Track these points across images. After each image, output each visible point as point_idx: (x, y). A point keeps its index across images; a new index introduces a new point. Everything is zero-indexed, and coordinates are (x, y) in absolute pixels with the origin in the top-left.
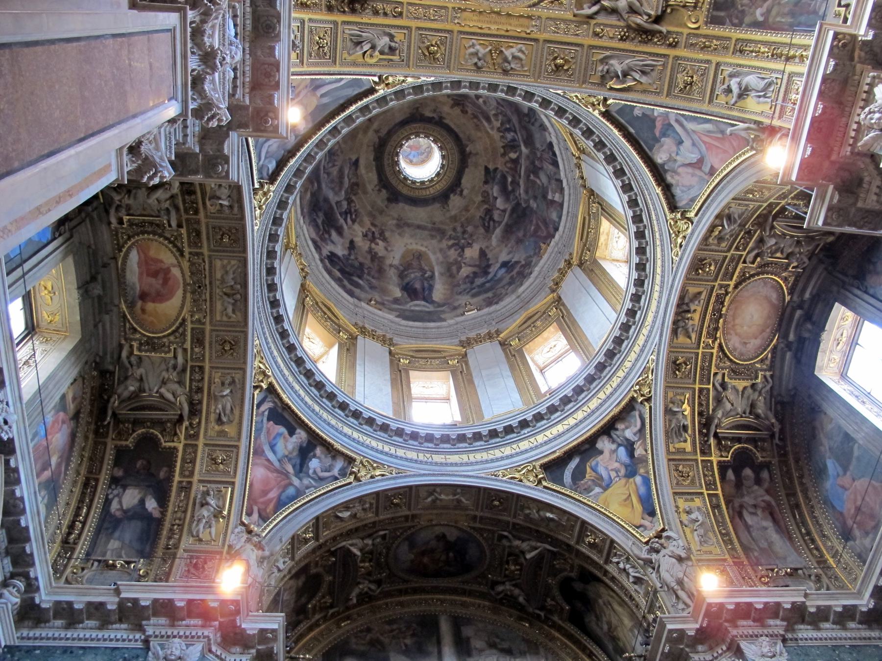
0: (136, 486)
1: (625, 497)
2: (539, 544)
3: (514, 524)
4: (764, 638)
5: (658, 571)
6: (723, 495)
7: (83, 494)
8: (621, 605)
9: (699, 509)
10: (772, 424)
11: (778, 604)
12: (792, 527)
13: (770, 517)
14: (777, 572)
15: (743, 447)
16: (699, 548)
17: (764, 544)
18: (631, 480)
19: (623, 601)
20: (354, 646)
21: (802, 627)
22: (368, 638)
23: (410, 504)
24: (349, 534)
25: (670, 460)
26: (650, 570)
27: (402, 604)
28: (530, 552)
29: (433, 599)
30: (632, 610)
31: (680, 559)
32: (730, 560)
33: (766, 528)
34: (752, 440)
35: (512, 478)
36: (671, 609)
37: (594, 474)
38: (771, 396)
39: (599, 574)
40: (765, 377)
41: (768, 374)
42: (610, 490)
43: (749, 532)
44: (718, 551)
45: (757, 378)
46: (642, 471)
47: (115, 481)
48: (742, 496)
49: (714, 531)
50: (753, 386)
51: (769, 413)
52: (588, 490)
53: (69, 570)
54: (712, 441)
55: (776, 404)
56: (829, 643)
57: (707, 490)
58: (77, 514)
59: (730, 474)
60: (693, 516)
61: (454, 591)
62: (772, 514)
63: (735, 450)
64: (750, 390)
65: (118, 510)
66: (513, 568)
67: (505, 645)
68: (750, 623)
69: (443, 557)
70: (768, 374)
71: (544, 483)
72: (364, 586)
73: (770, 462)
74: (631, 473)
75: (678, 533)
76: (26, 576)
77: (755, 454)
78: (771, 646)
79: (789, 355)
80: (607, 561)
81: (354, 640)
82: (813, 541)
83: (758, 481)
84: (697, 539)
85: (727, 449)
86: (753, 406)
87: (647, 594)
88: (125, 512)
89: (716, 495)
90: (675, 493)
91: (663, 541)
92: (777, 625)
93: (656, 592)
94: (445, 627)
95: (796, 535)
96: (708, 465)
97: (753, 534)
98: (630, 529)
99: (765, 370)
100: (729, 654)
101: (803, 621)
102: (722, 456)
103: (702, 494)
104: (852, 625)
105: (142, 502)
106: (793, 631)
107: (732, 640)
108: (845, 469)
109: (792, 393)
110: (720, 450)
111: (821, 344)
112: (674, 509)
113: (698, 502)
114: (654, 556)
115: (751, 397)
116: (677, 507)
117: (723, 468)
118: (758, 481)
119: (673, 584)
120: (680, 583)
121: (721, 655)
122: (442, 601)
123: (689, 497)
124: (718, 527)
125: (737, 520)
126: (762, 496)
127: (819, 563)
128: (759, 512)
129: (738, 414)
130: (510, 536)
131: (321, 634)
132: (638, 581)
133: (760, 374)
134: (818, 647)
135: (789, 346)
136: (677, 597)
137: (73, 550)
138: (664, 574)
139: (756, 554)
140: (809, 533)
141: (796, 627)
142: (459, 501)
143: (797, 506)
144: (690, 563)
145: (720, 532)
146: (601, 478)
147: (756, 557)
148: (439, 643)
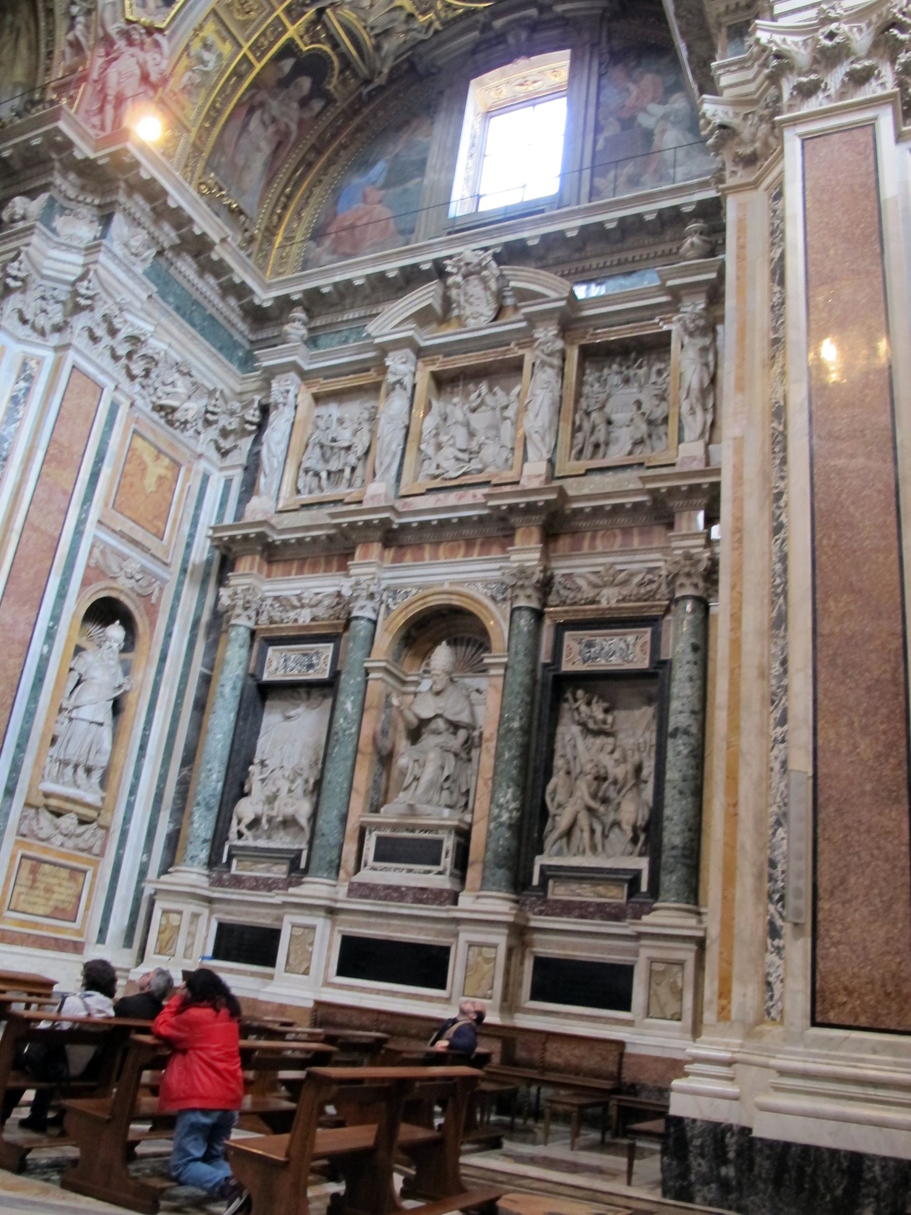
4: (145, 232)
5: (109, 63)
6: (258, 74)
8: (30, 48)
9: (220, 56)
10: (380, 73)
11: (190, 221)
12: (282, 176)
13: (274, 146)
14: (222, 196)
15: (329, 57)
16: (176, 90)
17: (240, 161)
19: (38, 48)
26: (101, 51)
30: (37, 68)
31: (145, 78)
32: (193, 135)
33: (259, 149)
34: (346, 62)
36: (82, 112)
38: (412, 48)
40: (431, 24)
41: (437, 25)
43: (240, 135)
44: (192, 115)
45: (424, 13)
48: (274, 96)
49: (209, 95)
50: (411, 16)
51: (391, 58)
54: (311, 12)
55: (408, 60)
57: (250, 48)
59: (288, 65)
60: (207, 56)
62: (279, 145)
63: (320, 49)
64: (402, 16)
68: (148, 208)
70: (437, 25)
73: (335, 101)
75: (173, 52)
77: (332, 76)
78: (143, 245)
79: (475, 34)
82: (285, 207)
83: (304, 103)
84: (185, 80)
85: (315, 39)
86: (387, 33)
87: (72, 70)
89: (251, 66)
90: (214, 12)
91: (148, 40)
92: (169, 235)
93: (84, 78)
95: (276, 186)
96: (278, 28)
97: (242, 141)
99: (439, 18)
100: (95, 211)
101: (196, 256)
102: (301, 37)
106: (178, 255)
107: (113, 204)
108: (386, 185)
109: (433, 70)
110: (307, 31)
111: (510, 66)
112: (195, 25)
113: (227, 48)
114: (121, 44)
115: (396, 24)
116: (201, 27)
117: (289, 49)
118: (304, 103)
119: (111, 92)
120: (120, 101)
121: (87, 204)
123: (224, 33)
124: (218, 95)
125: (244, 111)
126: (291, 119)
127: (267, 229)
128: (271, 129)
129: (364, 21)
132: (76, 46)
133: (431, 15)
135: (486, 27)
136: (101, 110)
138: (112, 74)
139: (223, 159)
140: (290, 197)
141: (184, 254)
143: (310, 165)
144: (151, 93)
145: (214, 102)
147: (219, 162)
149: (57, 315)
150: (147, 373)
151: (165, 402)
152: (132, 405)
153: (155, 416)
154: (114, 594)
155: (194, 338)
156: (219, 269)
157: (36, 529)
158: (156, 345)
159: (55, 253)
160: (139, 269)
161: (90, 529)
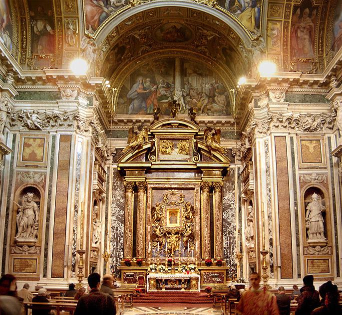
0: (41, 20)
1: (250, 17)
2: (213, 33)
3: (203, 24)
7: (22, 25)
18: (253, 9)
20: (142, 72)
21: (296, 87)
22: (147, 68)
23: (158, 16)
24: (133, 30)
25: (269, 3)
27: (160, 53)
28: (210, 36)
29: (173, 51)
35: (203, 3)
37: (238, 3)
39: (234, 48)
42: (243, 13)
44: (279, 49)
46: (258, 5)
47: (32, 18)
49: (281, 40)
52: (235, 11)
53: (27, 60)
56: (304, 93)
58: (23, 35)
61: (183, 48)
65: (37, 31)
66: (204, 41)
67: (200, 72)
69: (176, 35)
71: (217, 7)
72: (144, 47)
74: (253, 6)
75: (264, 39)
76: (12, 70)
80: (238, 46)
81: (142, 69)
88: (40, 32)
92: (286, 86)
94: (177, 63)
97: (298, 41)
98: (248, 33)
103: (281, 21)
104: (316, 86)
105: (45, 27)
116: (268, 27)
122: (178, 52)
123: (275, 22)
125: (294, 34)
130: (202, 29)
131: (129, 67)
134: (299, 94)
137: (26, 51)
142: (179, 14)
143: (323, 29)
145: (283, 40)
146: (241, 6)
148: (174, 70)
149: (266, 126)
150: (298, 124)
151: (307, 127)
152: (297, 134)
153: (306, 132)
154: (312, 186)
155: (308, 105)
156: (305, 82)
157: (281, 181)
158: (296, 116)
159: (261, 112)
160: (282, 101)
161: (297, 172)
